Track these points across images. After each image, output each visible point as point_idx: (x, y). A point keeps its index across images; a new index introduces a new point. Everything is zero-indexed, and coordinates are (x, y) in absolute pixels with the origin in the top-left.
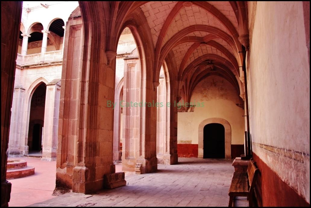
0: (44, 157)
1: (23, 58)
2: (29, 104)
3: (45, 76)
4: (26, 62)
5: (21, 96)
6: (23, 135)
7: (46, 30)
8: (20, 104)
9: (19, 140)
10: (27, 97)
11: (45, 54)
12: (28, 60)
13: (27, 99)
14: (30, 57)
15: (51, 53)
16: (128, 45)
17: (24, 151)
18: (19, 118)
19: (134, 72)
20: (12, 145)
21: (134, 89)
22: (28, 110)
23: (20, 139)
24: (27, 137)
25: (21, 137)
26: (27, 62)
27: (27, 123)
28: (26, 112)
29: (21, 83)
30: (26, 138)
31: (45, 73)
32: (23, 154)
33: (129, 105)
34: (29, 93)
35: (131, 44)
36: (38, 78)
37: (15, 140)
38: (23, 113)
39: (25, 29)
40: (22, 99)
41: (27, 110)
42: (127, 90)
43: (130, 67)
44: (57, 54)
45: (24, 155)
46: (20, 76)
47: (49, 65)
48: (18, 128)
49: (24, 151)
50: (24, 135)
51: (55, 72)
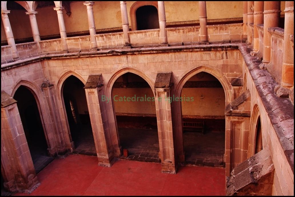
0: (101, 162)
1: (38, 44)
2: (62, 100)
3: (75, 70)
4: (43, 49)
5: (52, 94)
6: (66, 132)
7: (60, 7)
8: (53, 103)
9: (63, 139)
10: (58, 93)
11: (66, 40)
12: (46, 47)
13: (58, 95)
14: (47, 44)
15: (74, 39)
16: (184, 32)
17: (72, 149)
18: (56, 117)
19: (239, 129)
20: (58, 145)
21: (239, 149)
22: (63, 106)
23: (64, 137)
24: (70, 133)
25: (63, 135)
26: (45, 49)
27: (66, 120)
28: (61, 109)
29: (46, 76)
30: (69, 135)
31: (74, 65)
32: (72, 151)
33: (233, 166)
34: (59, 88)
35: (189, 32)
36: (66, 72)
37: (60, 142)
38: (58, 110)
39: (28, 5)
40: (54, 96)
41: (62, 107)
42: (231, 150)
43: (234, 123)
44: (84, 40)
45: (73, 151)
46: (42, 69)
47: (77, 57)
48: (59, 128)
49: (72, 149)
50: (66, 133)
51: (88, 65)
